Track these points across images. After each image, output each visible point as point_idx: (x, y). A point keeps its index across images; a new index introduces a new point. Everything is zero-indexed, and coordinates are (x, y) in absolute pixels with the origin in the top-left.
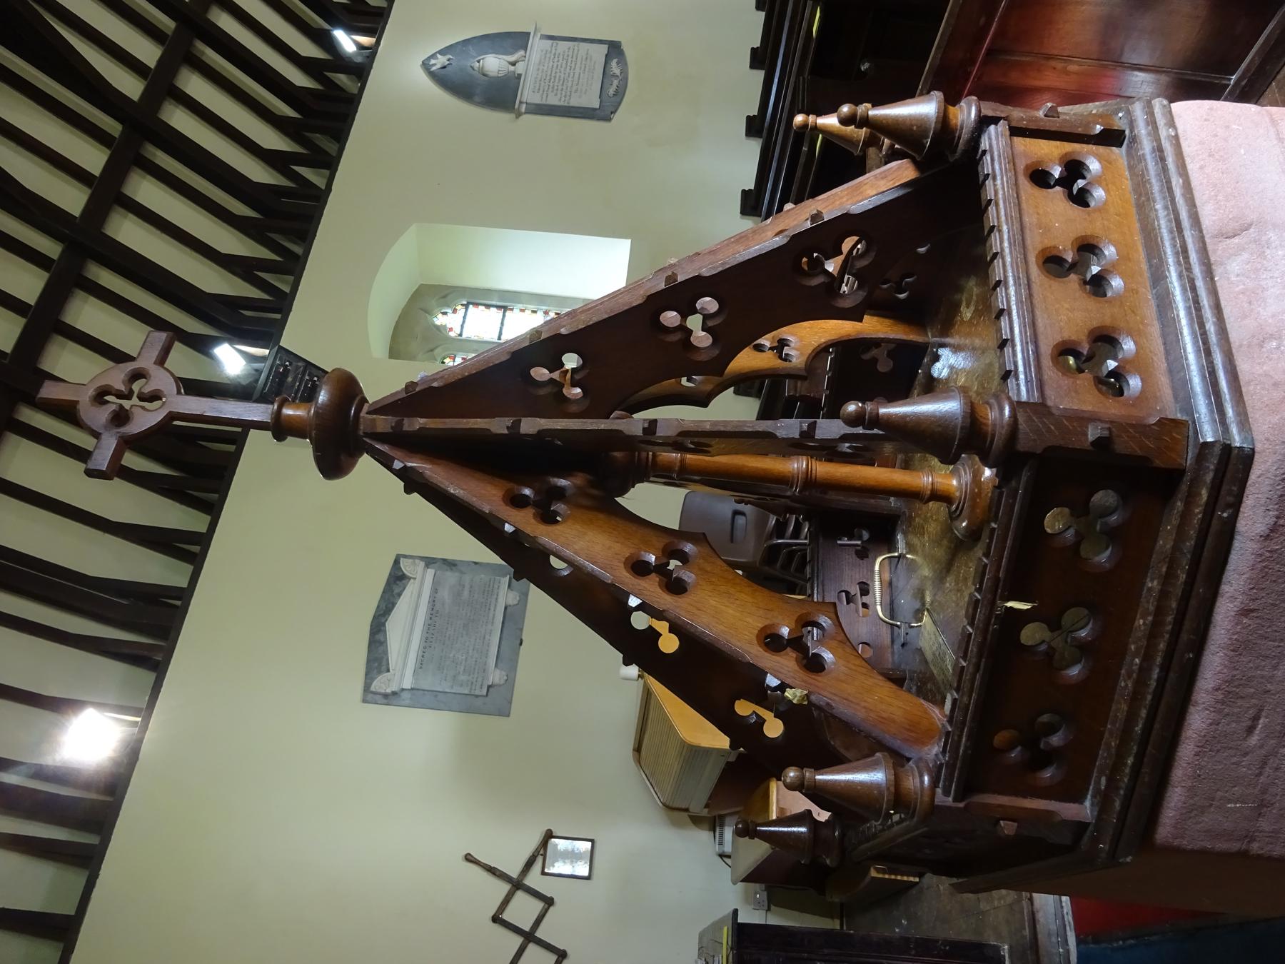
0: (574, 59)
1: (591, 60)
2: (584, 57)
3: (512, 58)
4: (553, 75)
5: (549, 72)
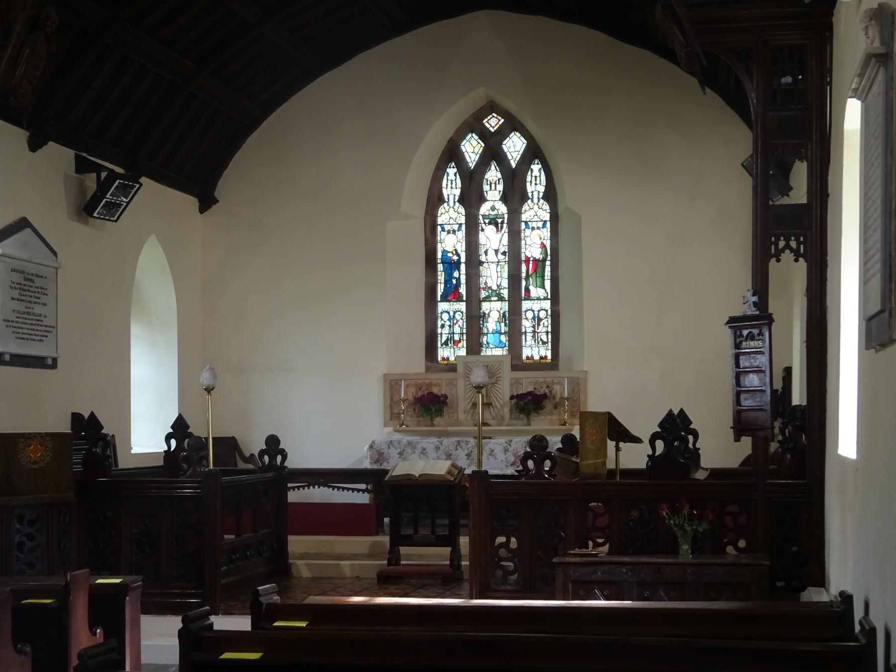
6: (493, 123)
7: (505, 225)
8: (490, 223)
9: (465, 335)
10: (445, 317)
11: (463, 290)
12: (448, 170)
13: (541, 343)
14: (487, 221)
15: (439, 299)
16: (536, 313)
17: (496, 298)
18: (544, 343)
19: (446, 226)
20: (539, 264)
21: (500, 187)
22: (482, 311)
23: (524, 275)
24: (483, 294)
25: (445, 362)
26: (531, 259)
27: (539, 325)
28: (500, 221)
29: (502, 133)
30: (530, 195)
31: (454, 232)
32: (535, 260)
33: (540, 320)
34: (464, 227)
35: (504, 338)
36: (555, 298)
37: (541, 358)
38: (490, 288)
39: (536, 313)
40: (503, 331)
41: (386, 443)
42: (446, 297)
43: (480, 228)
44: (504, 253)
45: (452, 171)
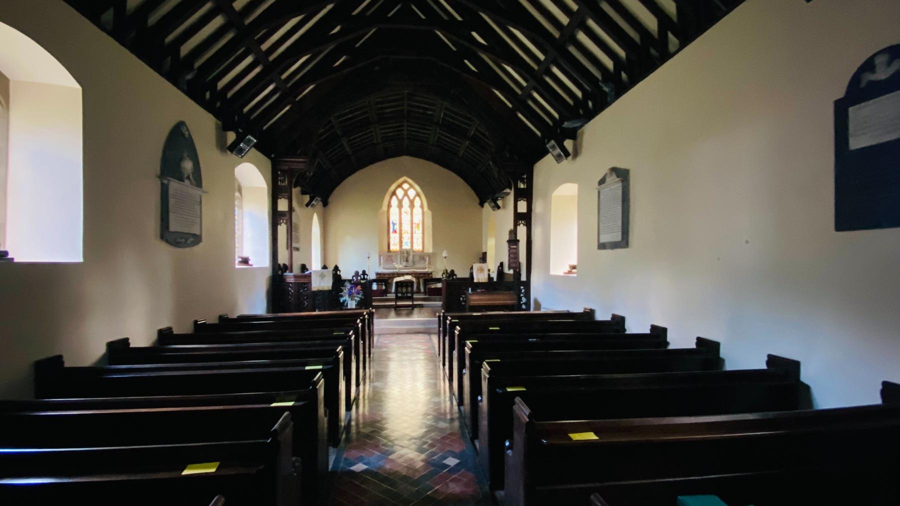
3: (191, 177)
6: (406, 186)
20: (418, 225)
24: (403, 232)
32: (417, 224)
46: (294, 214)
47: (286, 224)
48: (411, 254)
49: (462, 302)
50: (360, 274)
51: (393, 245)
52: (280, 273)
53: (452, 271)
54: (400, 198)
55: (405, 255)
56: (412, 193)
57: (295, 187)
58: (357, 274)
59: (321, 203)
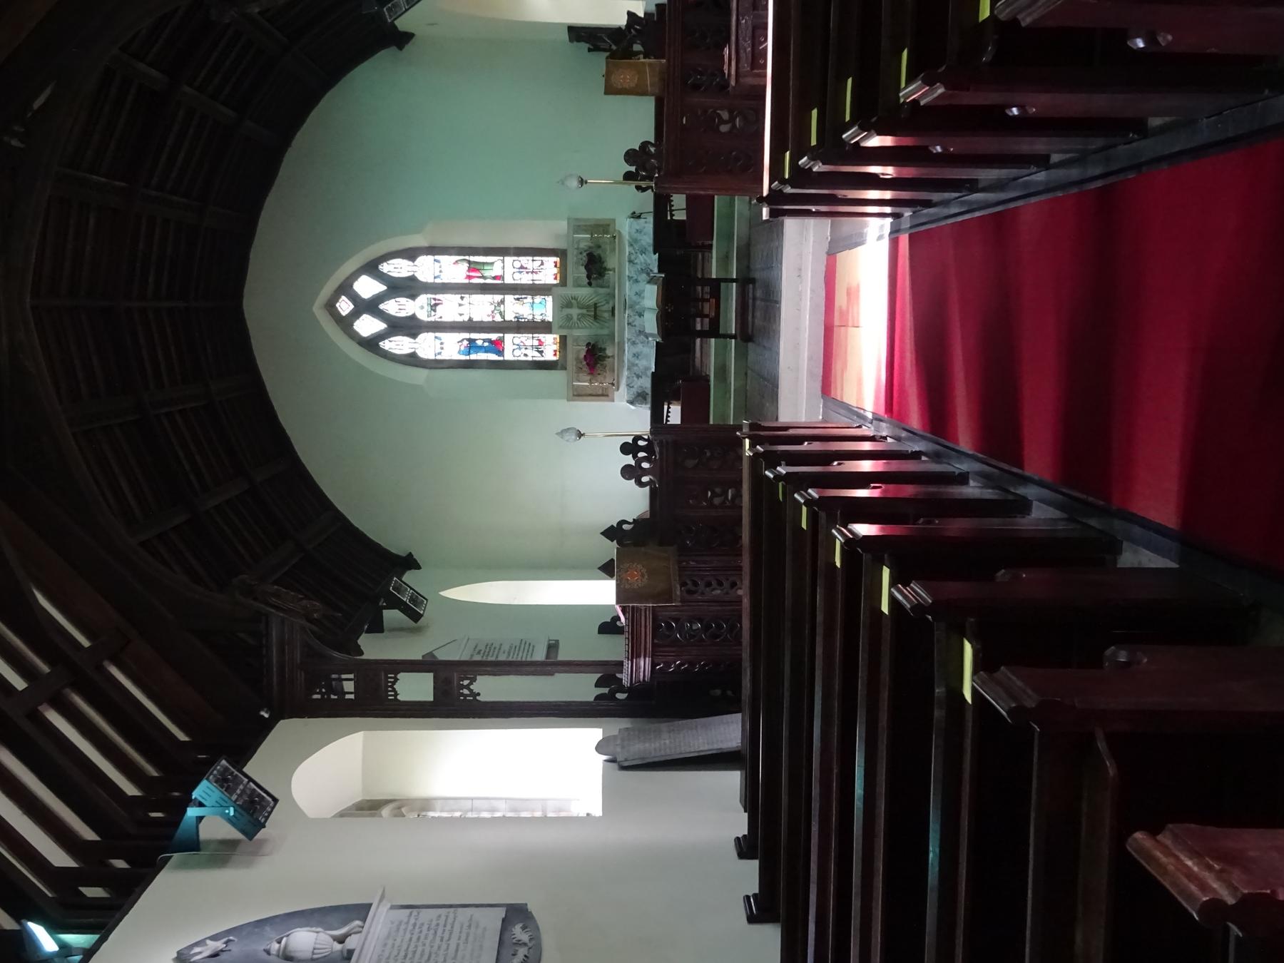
0: (448, 927)
1: (477, 927)
2: (466, 924)
4: (411, 949)
5: (405, 947)
6: (345, 306)
7: (438, 296)
8: (435, 311)
9: (535, 335)
10: (517, 353)
11: (494, 336)
12: (386, 348)
13: (542, 267)
14: (433, 313)
15: (501, 358)
16: (516, 270)
17: (502, 306)
18: (542, 264)
19: (437, 352)
20: (473, 267)
21: (403, 300)
22: (513, 320)
23: (482, 281)
24: (498, 318)
25: (558, 353)
26: (468, 274)
27: (526, 268)
28: (433, 302)
29: (354, 298)
30: (411, 274)
31: (442, 344)
32: (470, 270)
33: (522, 267)
34: (438, 334)
35: (538, 299)
36: (502, 252)
37: (556, 266)
38: (493, 312)
39: (516, 270)
40: (531, 301)
41: (628, 389)
42: (500, 351)
43: (439, 320)
44: (462, 298)
45: (386, 345)
46: (442, 656)
47: (473, 680)
48: (570, 291)
49: (734, 126)
50: (633, 463)
51: (541, 352)
52: (620, 696)
53: (630, 156)
54: (382, 288)
55: (575, 312)
56: (367, 287)
57: (362, 653)
58: (627, 472)
59: (409, 577)
